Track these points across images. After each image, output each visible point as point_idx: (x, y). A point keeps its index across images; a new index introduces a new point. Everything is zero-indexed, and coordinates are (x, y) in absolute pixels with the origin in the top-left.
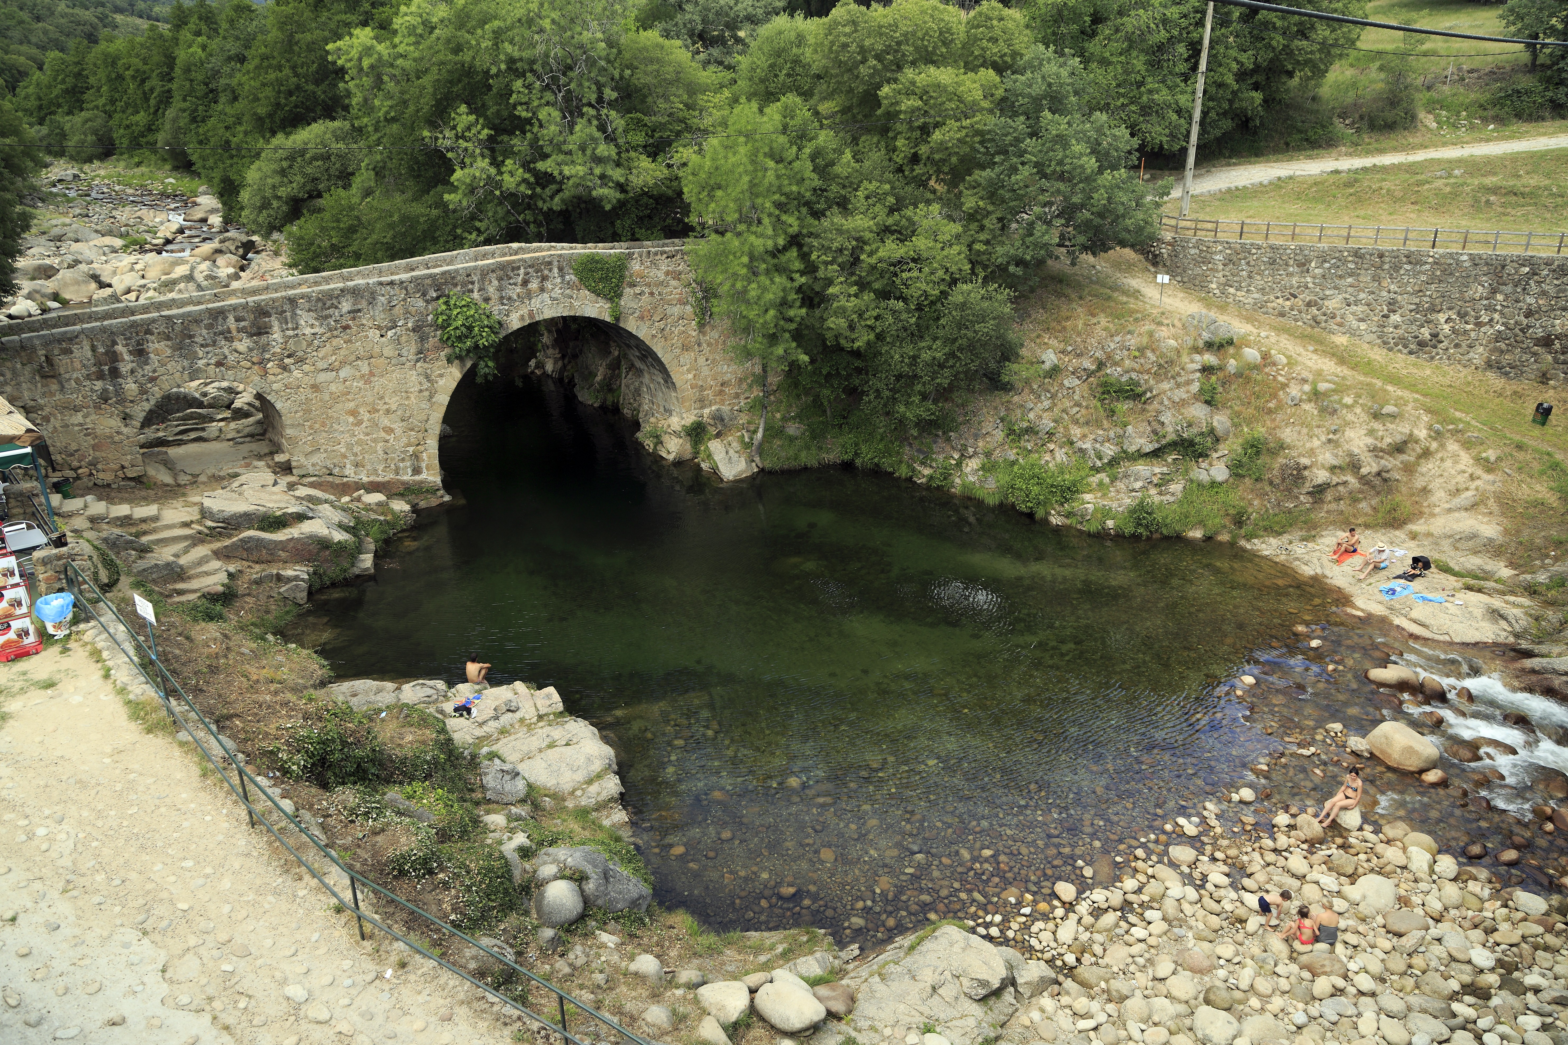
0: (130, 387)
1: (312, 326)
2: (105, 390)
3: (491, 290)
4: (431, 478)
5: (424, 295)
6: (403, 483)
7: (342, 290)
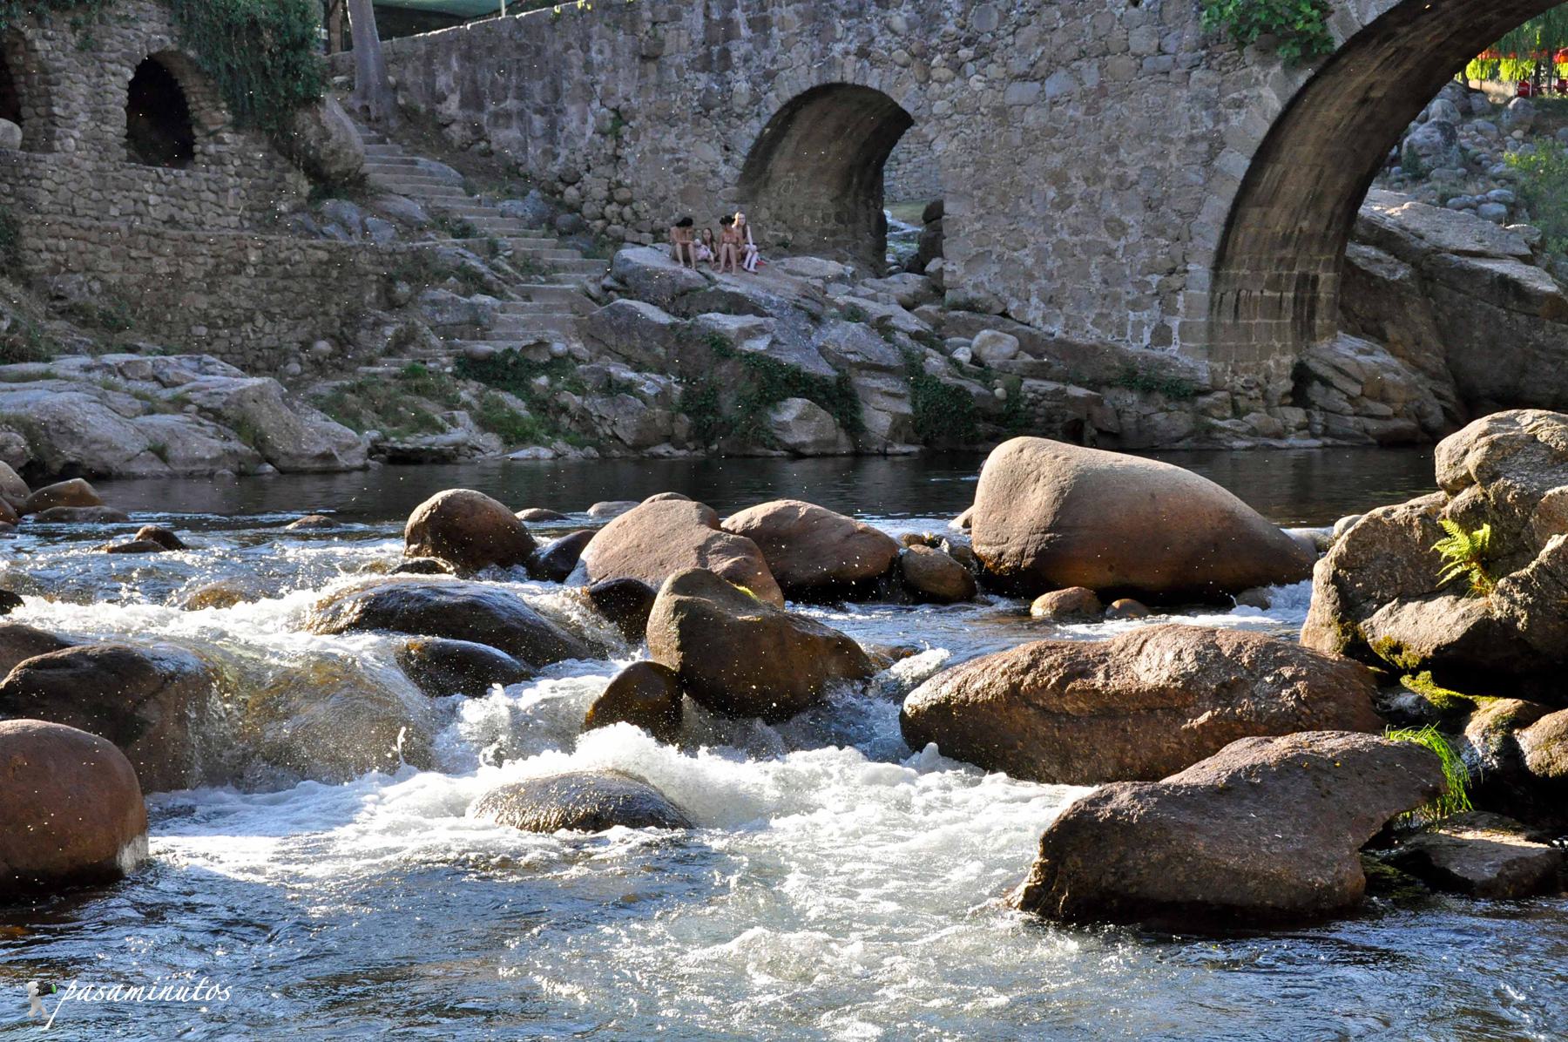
0: (742, 86)
4: (1187, 361)
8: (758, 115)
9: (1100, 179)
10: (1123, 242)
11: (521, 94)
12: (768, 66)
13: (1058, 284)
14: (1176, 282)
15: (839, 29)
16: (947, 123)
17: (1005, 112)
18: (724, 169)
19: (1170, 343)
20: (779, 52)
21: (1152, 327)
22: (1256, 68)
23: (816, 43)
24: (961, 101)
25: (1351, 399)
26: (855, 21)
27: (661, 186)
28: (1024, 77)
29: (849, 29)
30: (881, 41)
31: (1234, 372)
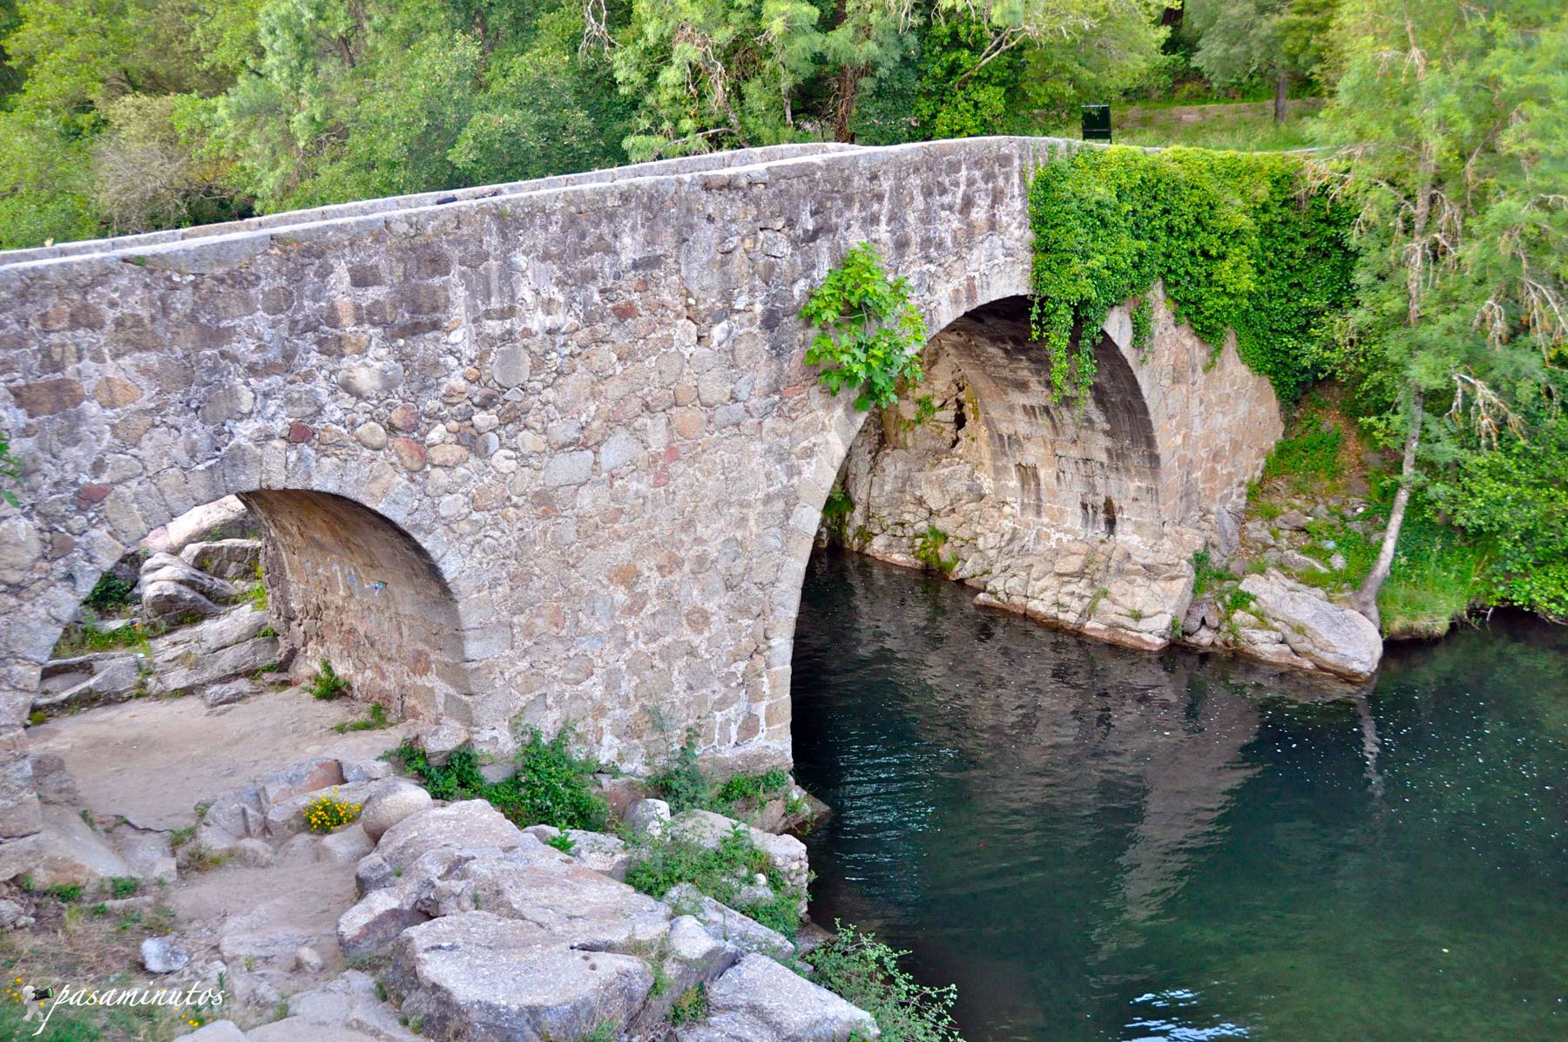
1: (548, 306)
3: (911, 218)
7: (625, 197)
8: (70, 577)
9: (679, 564)
10: (706, 634)
12: (84, 479)
14: (759, 662)
15: (246, 397)
17: (550, 499)
19: (756, 732)
20: (111, 450)
21: (739, 723)
22: (820, 413)
23: (198, 424)
26: (276, 380)
29: (266, 395)
30: (334, 411)
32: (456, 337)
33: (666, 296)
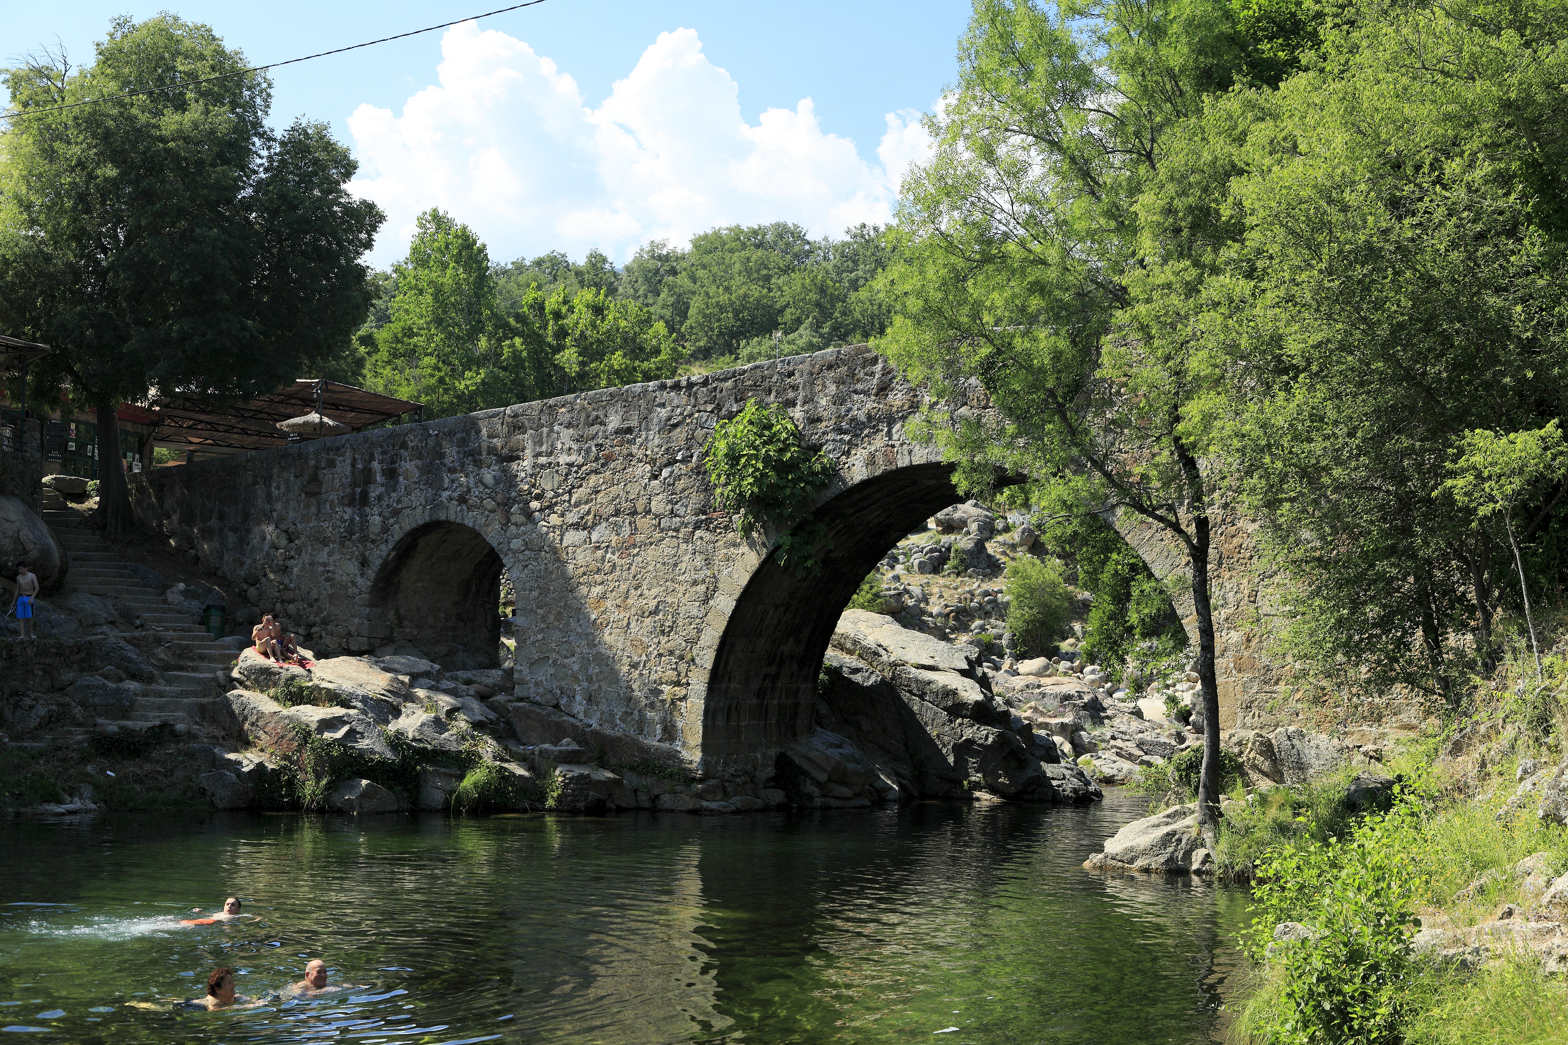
0: (376, 520)
2: (352, 520)
5: (719, 407)
6: (643, 750)
11: (222, 517)
13: (596, 687)
15: (447, 480)
16: (521, 556)
18: (360, 581)
24: (531, 541)
25: (819, 785)
27: (315, 590)
28: (576, 526)
30: (475, 492)
31: (726, 764)
32: (525, 463)
33: (634, 449)
